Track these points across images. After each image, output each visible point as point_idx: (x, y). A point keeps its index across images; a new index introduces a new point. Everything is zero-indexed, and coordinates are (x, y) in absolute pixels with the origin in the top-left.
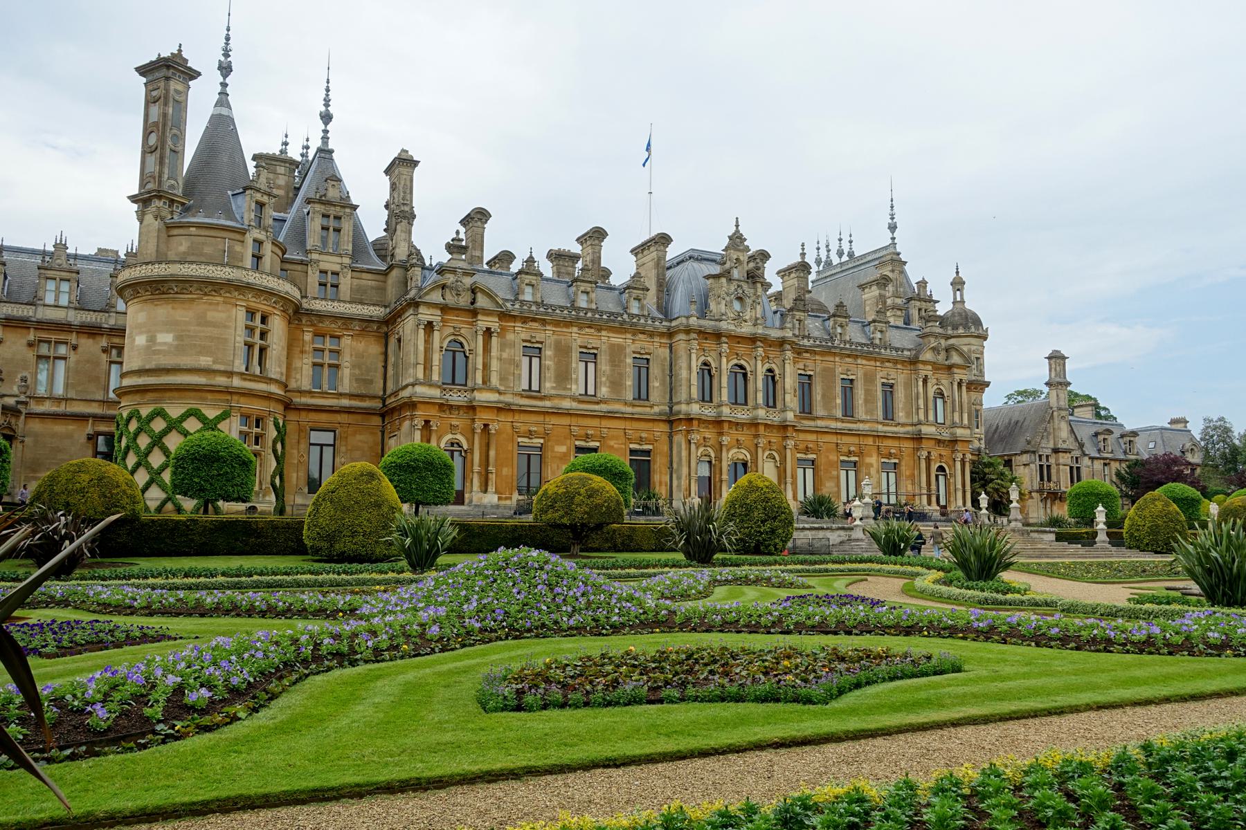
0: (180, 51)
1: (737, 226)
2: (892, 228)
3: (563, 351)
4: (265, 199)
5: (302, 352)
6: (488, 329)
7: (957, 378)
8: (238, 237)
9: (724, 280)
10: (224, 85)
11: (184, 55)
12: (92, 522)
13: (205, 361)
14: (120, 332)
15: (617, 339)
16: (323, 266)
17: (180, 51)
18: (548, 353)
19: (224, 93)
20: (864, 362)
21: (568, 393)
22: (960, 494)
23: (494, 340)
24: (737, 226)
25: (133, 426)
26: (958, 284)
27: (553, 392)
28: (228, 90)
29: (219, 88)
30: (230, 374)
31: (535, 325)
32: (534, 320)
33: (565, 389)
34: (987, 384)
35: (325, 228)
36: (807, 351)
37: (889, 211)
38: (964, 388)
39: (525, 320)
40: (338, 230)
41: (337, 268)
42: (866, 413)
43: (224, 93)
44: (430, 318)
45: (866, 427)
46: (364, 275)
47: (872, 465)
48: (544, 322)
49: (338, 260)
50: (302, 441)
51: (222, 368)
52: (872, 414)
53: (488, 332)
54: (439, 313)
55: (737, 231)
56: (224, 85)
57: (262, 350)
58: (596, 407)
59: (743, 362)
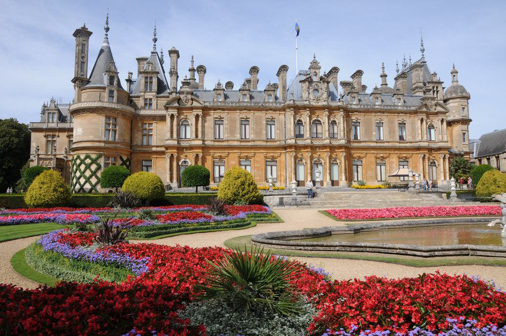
2: (423, 51)
3: (232, 121)
5: (138, 131)
7: (441, 118)
9: (307, 83)
13: (91, 138)
14: (71, 130)
15: (258, 114)
16: (146, 97)
18: (225, 122)
21: (236, 139)
22: (442, 175)
23: (200, 119)
25: (78, 162)
26: (454, 73)
27: (229, 139)
30: (100, 142)
31: (220, 111)
32: (219, 109)
33: (236, 137)
34: (471, 120)
35: (146, 82)
36: (356, 111)
37: (420, 42)
38: (445, 123)
39: (215, 109)
40: (151, 83)
41: (151, 97)
42: (390, 138)
44: (172, 113)
45: (390, 145)
46: (162, 99)
47: (393, 162)
48: (223, 110)
49: (150, 94)
50: (139, 165)
51: (97, 139)
53: (197, 117)
57: (115, 131)
59: (319, 119)
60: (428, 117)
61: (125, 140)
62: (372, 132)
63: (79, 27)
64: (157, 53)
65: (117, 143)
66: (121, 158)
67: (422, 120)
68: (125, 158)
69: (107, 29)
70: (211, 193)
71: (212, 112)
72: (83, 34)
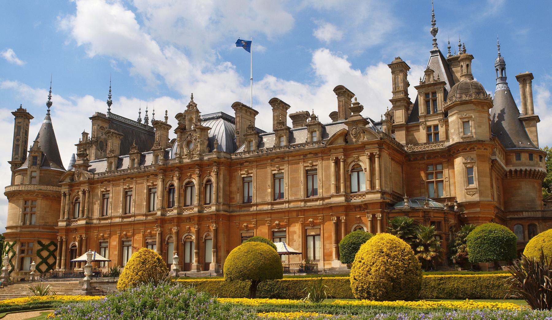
0: (21, 107)
1: (192, 98)
4: (37, 154)
6: (84, 190)
8: (25, 172)
10: (49, 111)
17: (21, 107)
20: (290, 158)
24: (192, 98)
29: (47, 112)
32: (106, 181)
33: (118, 212)
36: (246, 162)
39: (102, 182)
47: (295, 232)
48: (109, 181)
52: (296, 195)
53: (84, 193)
55: (192, 101)
56: (49, 111)
58: (130, 219)
60: (346, 156)
61: (48, 223)
62: (266, 189)
65: (35, 227)
66: (40, 243)
67: (337, 162)
68: (46, 242)
72: (22, 117)
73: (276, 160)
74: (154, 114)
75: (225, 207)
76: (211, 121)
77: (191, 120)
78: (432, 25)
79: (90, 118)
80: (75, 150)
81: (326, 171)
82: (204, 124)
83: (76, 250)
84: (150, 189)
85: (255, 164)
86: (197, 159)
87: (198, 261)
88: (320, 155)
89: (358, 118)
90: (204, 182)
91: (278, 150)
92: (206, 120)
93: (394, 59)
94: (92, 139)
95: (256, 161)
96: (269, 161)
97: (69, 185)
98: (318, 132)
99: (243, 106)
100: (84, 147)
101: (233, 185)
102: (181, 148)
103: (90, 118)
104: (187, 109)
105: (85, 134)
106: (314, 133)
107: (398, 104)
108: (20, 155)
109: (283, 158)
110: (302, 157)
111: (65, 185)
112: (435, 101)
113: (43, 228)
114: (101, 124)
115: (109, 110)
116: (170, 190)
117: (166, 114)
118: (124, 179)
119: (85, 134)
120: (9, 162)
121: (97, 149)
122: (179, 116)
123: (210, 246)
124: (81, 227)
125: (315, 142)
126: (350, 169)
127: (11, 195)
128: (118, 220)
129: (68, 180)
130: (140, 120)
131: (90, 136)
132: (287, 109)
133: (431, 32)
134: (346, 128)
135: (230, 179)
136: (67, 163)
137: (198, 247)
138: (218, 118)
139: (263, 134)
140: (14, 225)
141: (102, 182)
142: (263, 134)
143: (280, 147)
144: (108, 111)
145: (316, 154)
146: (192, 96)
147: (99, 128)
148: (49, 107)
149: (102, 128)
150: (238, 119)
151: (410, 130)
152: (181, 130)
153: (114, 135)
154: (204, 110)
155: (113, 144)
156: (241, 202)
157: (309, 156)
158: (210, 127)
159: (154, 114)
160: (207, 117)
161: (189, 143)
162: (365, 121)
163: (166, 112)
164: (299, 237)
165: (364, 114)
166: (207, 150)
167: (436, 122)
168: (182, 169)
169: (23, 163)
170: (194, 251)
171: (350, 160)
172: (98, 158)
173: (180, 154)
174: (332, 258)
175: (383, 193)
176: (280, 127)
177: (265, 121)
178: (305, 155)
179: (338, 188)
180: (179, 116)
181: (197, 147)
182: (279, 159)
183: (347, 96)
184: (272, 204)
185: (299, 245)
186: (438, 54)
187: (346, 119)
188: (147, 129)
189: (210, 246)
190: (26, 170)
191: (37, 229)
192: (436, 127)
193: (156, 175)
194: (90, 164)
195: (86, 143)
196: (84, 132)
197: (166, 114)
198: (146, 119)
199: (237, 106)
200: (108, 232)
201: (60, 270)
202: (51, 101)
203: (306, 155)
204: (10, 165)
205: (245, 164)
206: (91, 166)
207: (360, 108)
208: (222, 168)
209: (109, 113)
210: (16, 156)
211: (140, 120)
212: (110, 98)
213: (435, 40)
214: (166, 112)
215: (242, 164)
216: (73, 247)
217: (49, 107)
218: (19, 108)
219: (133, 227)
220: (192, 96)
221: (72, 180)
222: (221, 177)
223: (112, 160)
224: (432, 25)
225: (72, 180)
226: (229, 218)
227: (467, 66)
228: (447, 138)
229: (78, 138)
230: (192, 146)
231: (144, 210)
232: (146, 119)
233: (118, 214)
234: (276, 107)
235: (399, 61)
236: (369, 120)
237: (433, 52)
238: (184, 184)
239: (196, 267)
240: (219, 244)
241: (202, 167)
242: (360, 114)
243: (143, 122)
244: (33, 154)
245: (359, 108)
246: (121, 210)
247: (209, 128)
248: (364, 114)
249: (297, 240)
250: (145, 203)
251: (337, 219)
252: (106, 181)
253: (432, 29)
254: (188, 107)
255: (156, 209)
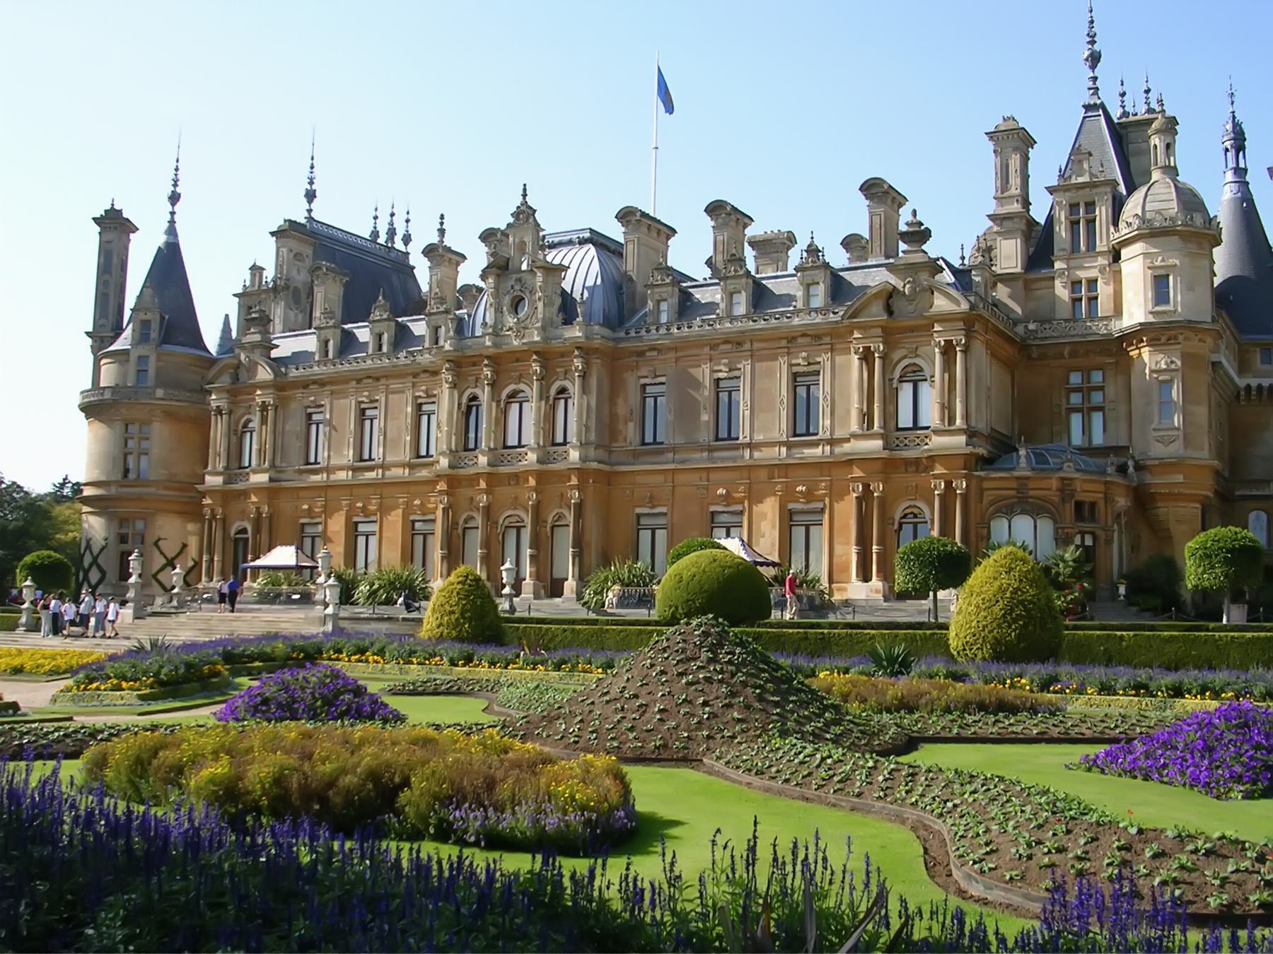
1: (525, 195)
4: (149, 316)
10: (173, 213)
11: (117, 207)
12: (573, 630)
19: (172, 222)
20: (756, 345)
24: (525, 195)
28: (176, 218)
29: (168, 217)
36: (652, 349)
43: (172, 222)
54: (225, 395)
55: (525, 203)
56: (173, 213)
63: (99, 212)
64: (1103, 106)
67: (867, 357)
69: (174, 198)
70: (1198, 629)
71: (299, 393)
72: (114, 226)
73: (722, 347)
74: (407, 221)
75: (601, 454)
76: (565, 250)
77: (521, 247)
78: (1089, 43)
79: (273, 234)
80: (232, 308)
81: (845, 380)
82: (554, 257)
83: (247, 539)
84: (421, 405)
85: (672, 355)
86: (537, 339)
87: (538, 576)
88: (827, 340)
89: (918, 258)
90: (553, 392)
91: (728, 325)
92: (553, 246)
93: (1001, 121)
94: (274, 281)
95: (676, 349)
96: (707, 349)
97: (228, 391)
98: (822, 286)
99: (644, 215)
100: (255, 304)
101: (620, 401)
102: (499, 311)
103: (273, 234)
104: (511, 220)
105: (256, 270)
106: (811, 288)
107: (1008, 224)
108: (111, 317)
109: (739, 344)
110: (784, 343)
111: (218, 390)
112: (1091, 222)
113: (166, 488)
114: (293, 244)
115: (310, 211)
116: (469, 409)
117: (442, 224)
118: (359, 381)
119: (256, 270)
120: (87, 333)
121: (288, 307)
122: (488, 236)
123: (565, 539)
124: (258, 489)
125: (816, 310)
126: (897, 374)
127: (91, 409)
128: (342, 475)
129: (225, 380)
130: (375, 234)
131: (269, 274)
132: (745, 226)
133: (1087, 60)
134: (893, 280)
135: (613, 389)
136: (212, 340)
137: (535, 544)
138: (582, 242)
139: (689, 284)
140: (103, 478)
141: (306, 386)
142: (689, 284)
143: (733, 319)
144: (306, 214)
145: (818, 337)
146: (525, 190)
147: (292, 255)
148: (173, 204)
149: (298, 256)
150: (630, 247)
151: (1034, 286)
152: (499, 268)
153: (331, 275)
154: (551, 222)
155: (327, 295)
156: (638, 440)
157: (800, 340)
158: (565, 263)
159: (407, 221)
160: (556, 240)
161: (516, 304)
162: (934, 267)
163: (442, 217)
164: (773, 527)
165: (932, 248)
166: (559, 319)
167: (1093, 273)
168: (504, 364)
169: (118, 336)
170: (527, 552)
171: (896, 355)
172: (292, 328)
173: (494, 327)
174: (850, 576)
175: (971, 434)
176: (726, 265)
177: (691, 253)
178: (792, 340)
179: (867, 417)
180: (488, 236)
181: (538, 309)
182: (729, 346)
183: (889, 201)
184: (711, 450)
185: (773, 545)
186: (1101, 112)
187: (887, 257)
188: (393, 255)
189: (565, 539)
190: (125, 352)
191: (152, 490)
192: (1092, 283)
193: (436, 373)
194: (274, 342)
195: (260, 291)
196: (254, 265)
197: (442, 224)
198: (392, 233)
199: (626, 216)
200: (320, 502)
201: (212, 585)
202: (178, 190)
203: (794, 338)
204: (89, 341)
205: (648, 354)
206: (277, 346)
207: (924, 235)
208: (596, 363)
209: (310, 219)
210: (103, 321)
211: (375, 234)
212: (311, 183)
213: (1095, 79)
214: (442, 217)
215: (641, 354)
216: (239, 532)
217: (173, 204)
218: (109, 207)
219: (379, 491)
220: (525, 190)
221: (236, 378)
222: (593, 382)
223: (329, 334)
224: (1089, 43)
225: (236, 378)
226: (608, 479)
227: (1168, 146)
228: (1118, 312)
229: (240, 279)
230: (525, 310)
231: (406, 455)
232: (392, 233)
233: (344, 462)
234: (720, 220)
235: (1011, 125)
236: (941, 262)
237: (1088, 108)
238: (504, 396)
239: (531, 589)
240: (587, 537)
241: (550, 359)
242: (924, 247)
243: (382, 240)
244: (142, 316)
245: (919, 235)
246: (351, 452)
247: (563, 268)
248: (932, 248)
249: (767, 535)
250: (408, 438)
251: (946, 486)
252: (314, 382)
253: (1087, 53)
254: (516, 215)
255: (432, 452)
